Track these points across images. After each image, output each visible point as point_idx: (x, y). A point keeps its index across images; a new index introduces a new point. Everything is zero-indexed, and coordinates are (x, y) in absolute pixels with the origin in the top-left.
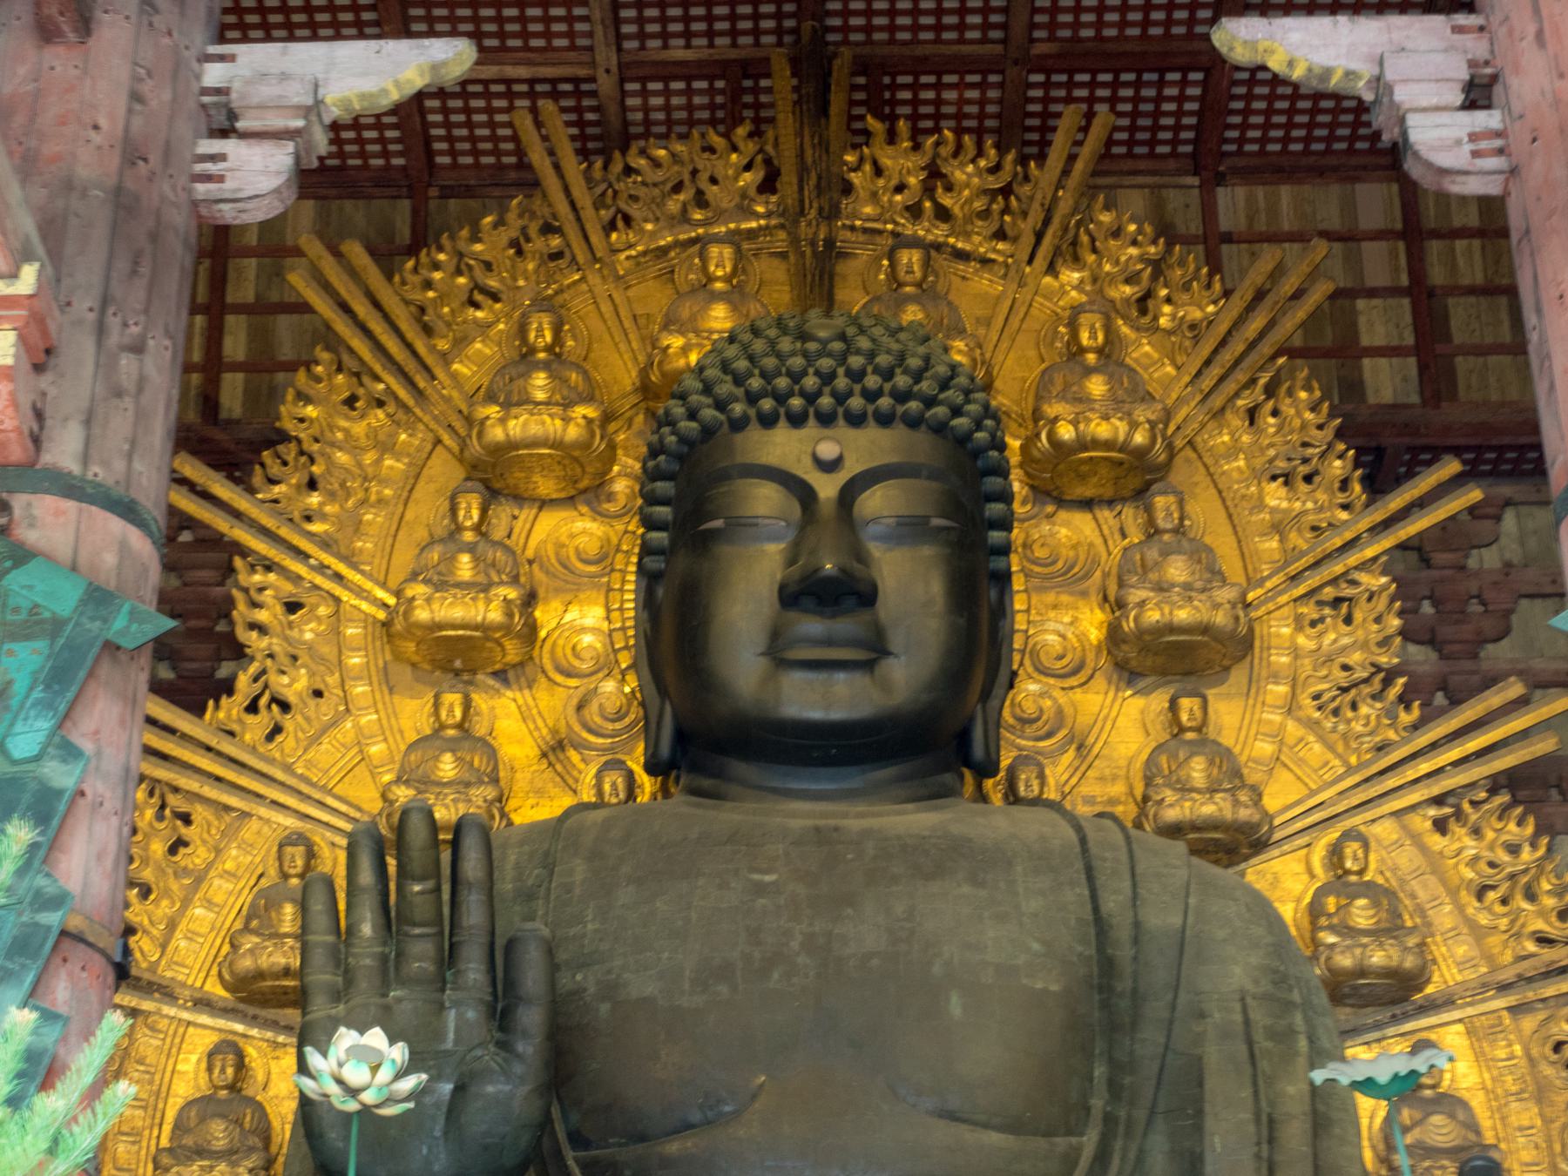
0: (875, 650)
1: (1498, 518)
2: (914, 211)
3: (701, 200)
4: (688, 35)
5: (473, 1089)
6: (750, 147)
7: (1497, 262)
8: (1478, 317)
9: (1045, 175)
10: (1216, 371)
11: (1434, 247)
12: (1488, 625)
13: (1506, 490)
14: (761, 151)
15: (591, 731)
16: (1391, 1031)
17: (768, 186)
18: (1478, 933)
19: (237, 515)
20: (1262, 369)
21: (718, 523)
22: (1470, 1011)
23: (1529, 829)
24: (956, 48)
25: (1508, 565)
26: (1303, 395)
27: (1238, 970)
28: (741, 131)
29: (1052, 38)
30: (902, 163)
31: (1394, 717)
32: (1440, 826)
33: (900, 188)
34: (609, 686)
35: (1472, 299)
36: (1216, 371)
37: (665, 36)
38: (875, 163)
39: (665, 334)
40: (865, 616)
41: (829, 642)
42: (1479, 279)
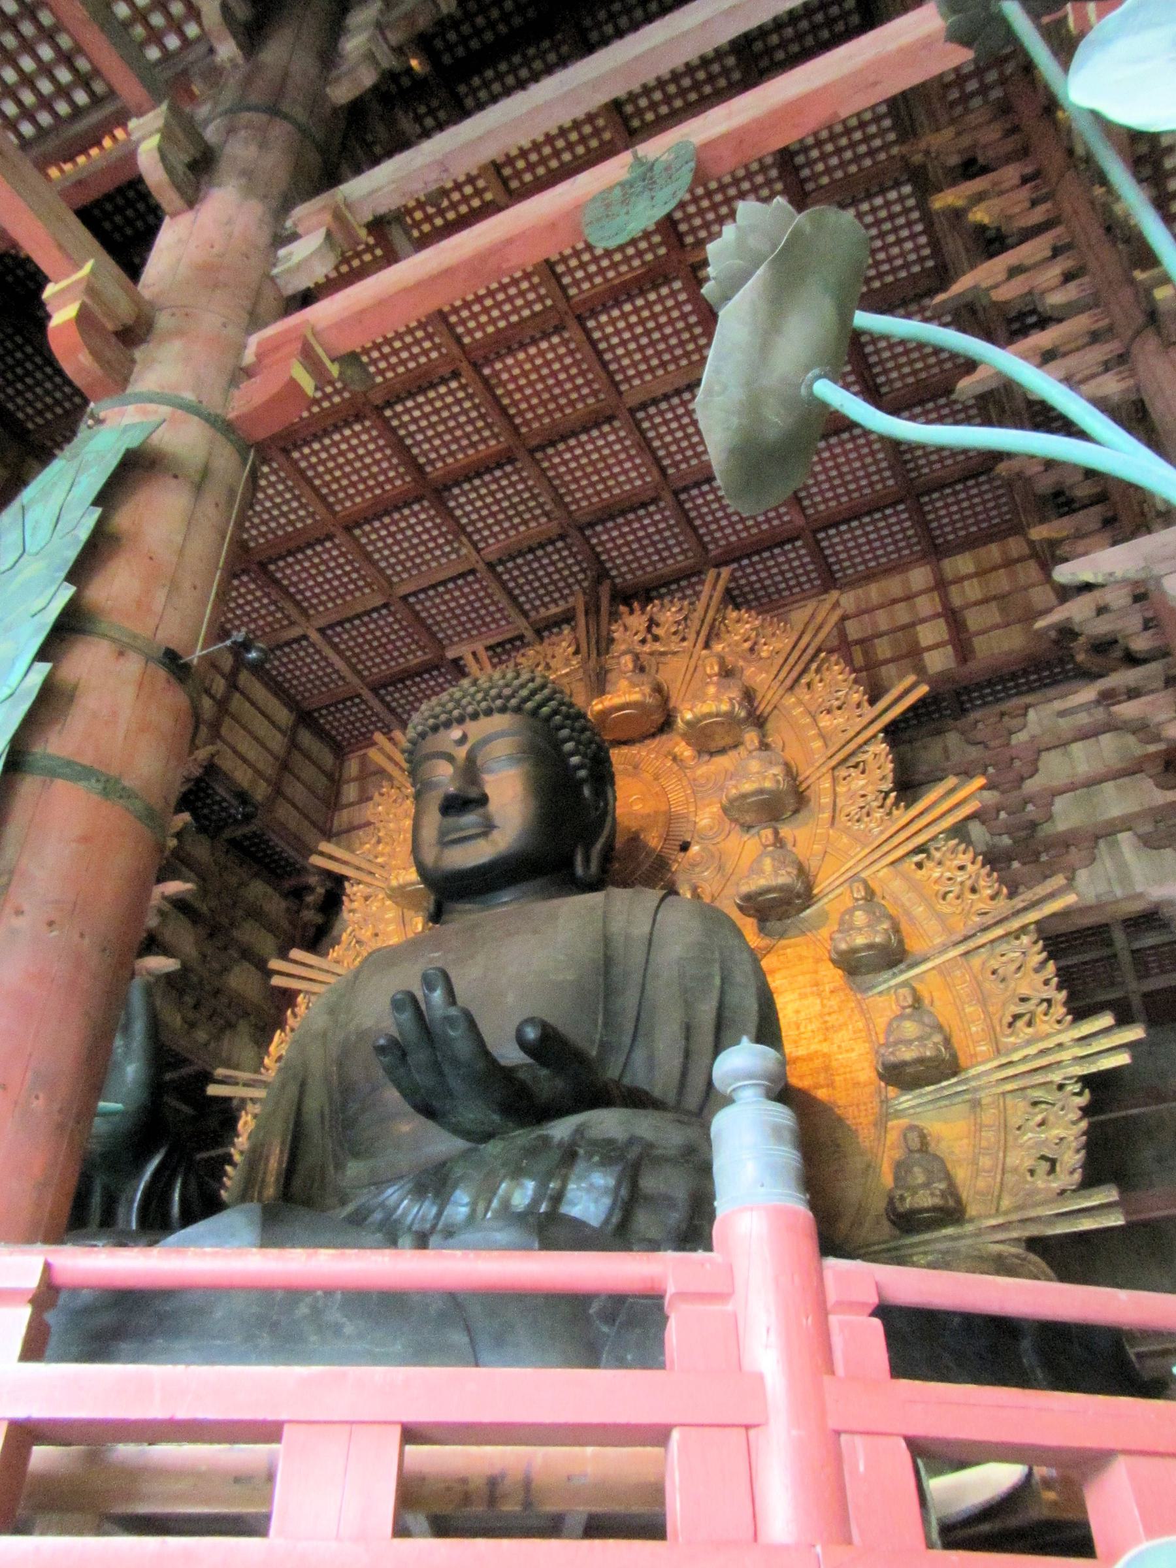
0: (488, 827)
1: (1025, 715)
2: (643, 641)
4: (555, 601)
9: (700, 606)
10: (786, 668)
11: (953, 589)
12: (1025, 771)
13: (1028, 699)
16: (893, 982)
17: (577, 652)
18: (941, 917)
19: (345, 863)
20: (812, 660)
22: (937, 961)
23: (970, 855)
25: (1033, 737)
30: (637, 621)
31: (889, 814)
32: (919, 865)
36: (786, 668)
37: (544, 605)
40: (481, 811)
42: (980, 596)
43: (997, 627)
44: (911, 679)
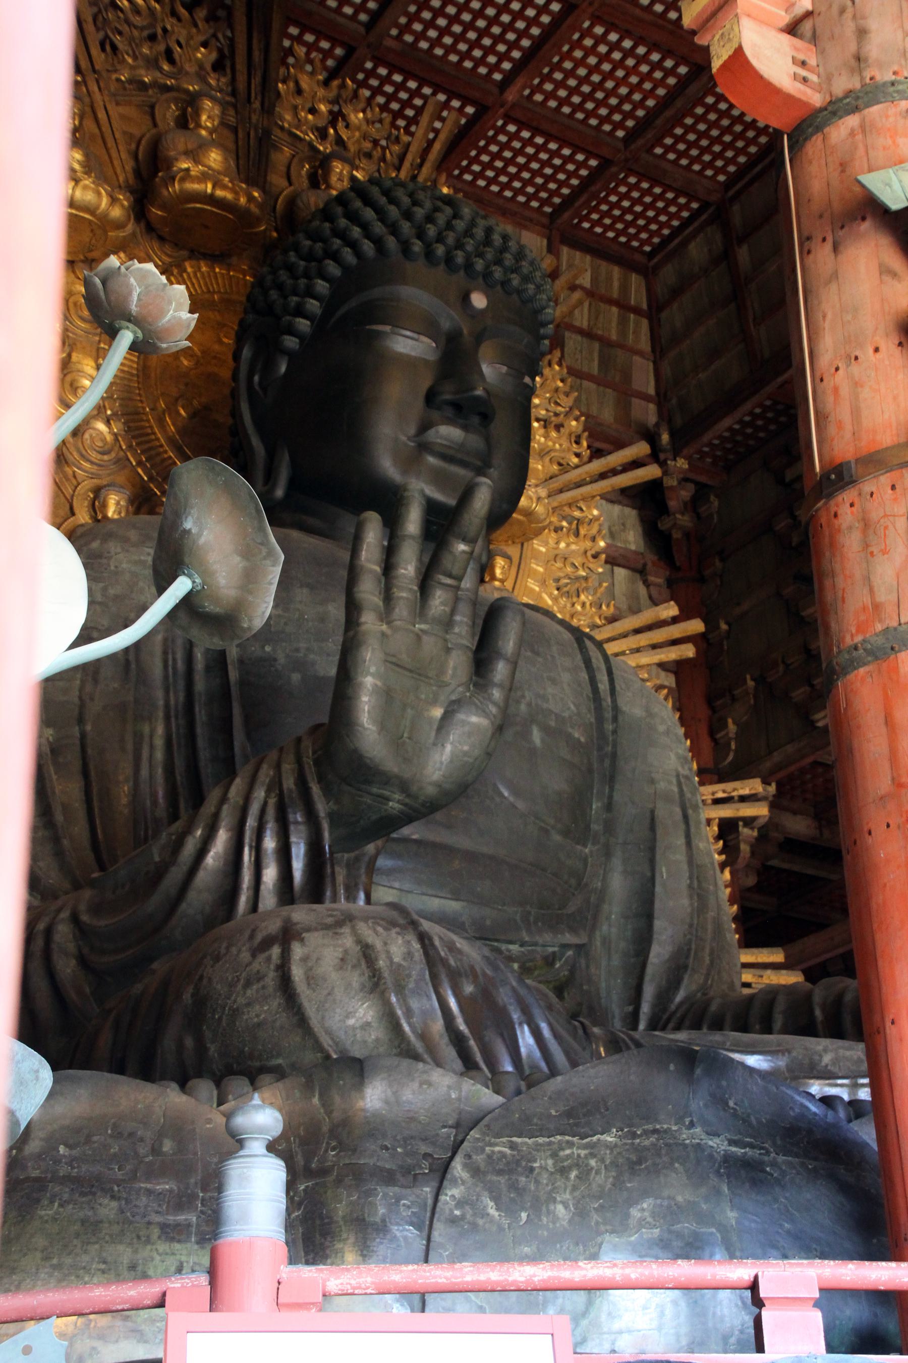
3: (169, 56)
5: (461, 716)
6: (205, 30)
7: (597, 318)
8: (581, 351)
14: (214, 36)
15: (82, 456)
17: (218, 66)
21: (387, 328)
24: (333, 16)
26: (557, 368)
27: (673, 756)
28: (201, 14)
29: (399, 37)
33: (313, 111)
34: (101, 426)
35: (579, 338)
38: (297, 83)
39: (183, 157)
41: (461, 446)
43: (590, 377)
44: (641, 449)
